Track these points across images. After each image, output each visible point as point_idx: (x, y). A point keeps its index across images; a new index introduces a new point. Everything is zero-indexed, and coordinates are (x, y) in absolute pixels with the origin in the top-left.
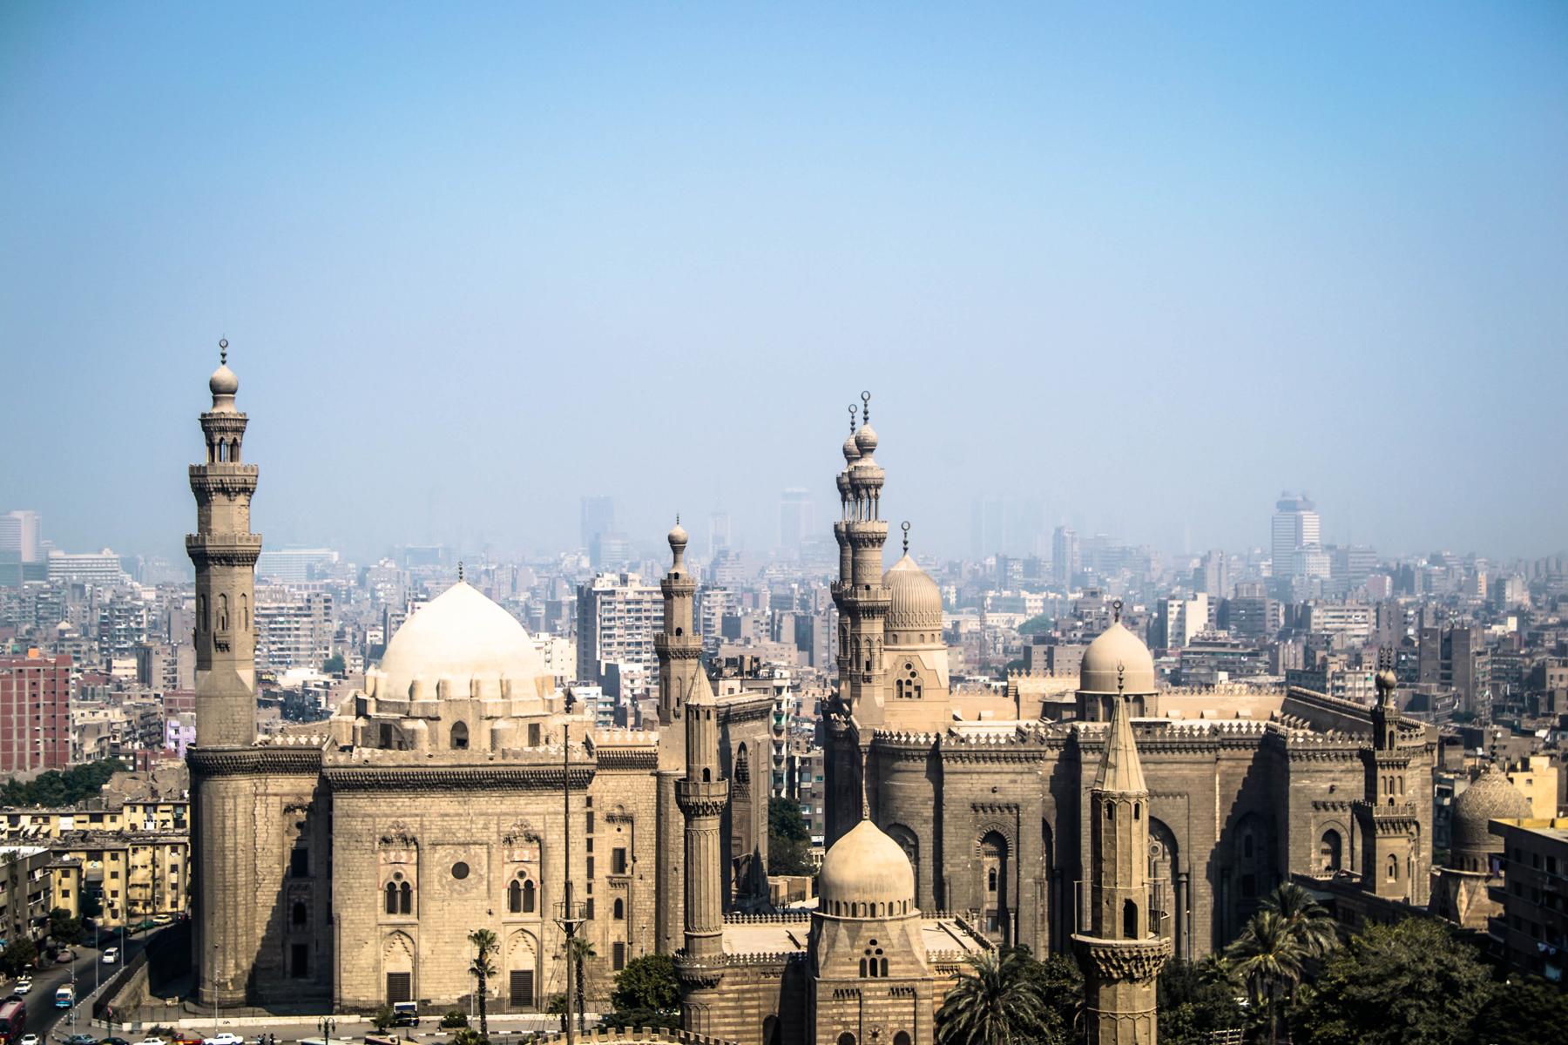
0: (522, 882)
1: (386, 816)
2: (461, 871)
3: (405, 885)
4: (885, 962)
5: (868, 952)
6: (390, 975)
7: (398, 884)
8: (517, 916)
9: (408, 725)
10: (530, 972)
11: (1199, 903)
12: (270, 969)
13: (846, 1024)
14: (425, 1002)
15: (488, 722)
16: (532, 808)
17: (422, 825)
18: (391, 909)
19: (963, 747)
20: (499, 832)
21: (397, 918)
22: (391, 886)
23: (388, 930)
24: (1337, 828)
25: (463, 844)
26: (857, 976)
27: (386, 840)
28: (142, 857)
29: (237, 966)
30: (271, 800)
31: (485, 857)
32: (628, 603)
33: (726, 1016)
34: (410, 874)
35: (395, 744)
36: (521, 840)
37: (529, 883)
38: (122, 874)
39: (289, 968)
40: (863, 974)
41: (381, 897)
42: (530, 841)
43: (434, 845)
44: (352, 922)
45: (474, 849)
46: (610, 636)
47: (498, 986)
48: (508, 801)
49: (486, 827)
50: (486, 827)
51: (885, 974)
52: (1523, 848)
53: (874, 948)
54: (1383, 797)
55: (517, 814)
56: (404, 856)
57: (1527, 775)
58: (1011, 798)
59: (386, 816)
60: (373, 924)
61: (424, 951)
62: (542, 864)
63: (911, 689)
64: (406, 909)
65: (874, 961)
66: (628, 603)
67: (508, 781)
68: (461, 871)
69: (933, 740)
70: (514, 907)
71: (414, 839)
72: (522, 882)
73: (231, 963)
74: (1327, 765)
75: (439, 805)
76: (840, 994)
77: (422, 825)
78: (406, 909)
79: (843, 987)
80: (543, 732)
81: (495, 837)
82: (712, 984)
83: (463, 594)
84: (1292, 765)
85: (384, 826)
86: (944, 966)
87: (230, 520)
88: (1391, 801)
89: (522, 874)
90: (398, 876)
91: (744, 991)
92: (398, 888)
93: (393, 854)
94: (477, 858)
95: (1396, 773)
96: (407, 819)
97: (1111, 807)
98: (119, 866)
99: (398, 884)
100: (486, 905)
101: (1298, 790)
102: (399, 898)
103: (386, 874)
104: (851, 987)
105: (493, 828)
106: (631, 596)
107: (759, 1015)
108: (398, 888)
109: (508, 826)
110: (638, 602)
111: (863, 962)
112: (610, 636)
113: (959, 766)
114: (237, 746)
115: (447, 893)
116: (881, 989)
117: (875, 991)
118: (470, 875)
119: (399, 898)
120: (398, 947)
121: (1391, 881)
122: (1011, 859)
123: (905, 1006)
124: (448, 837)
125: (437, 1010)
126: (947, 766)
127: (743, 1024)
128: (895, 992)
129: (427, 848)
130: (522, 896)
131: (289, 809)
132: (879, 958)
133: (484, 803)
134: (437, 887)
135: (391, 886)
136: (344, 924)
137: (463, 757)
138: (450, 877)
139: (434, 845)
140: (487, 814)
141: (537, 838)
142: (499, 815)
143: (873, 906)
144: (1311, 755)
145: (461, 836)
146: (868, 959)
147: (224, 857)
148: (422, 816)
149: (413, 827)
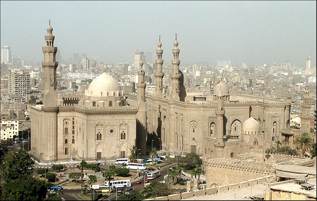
0: (123, 133)
1: (97, 120)
2: (112, 131)
3: (100, 134)
4: (258, 142)
5: (255, 140)
6: (97, 153)
9: (100, 102)
10: (124, 152)
12: (60, 153)
15: (116, 101)
16: (125, 119)
17: (104, 122)
18: (98, 140)
20: (119, 124)
23: (97, 143)
25: (112, 126)
26: (253, 145)
29: (55, 152)
30: (61, 118)
31: (116, 128)
33: (225, 153)
35: (96, 106)
39: (64, 153)
40: (254, 144)
43: (106, 126)
44: (90, 142)
46: (17, 84)
48: (121, 117)
49: (117, 122)
50: (117, 122)
53: (256, 140)
55: (123, 120)
59: (97, 120)
60: (95, 142)
61: (105, 148)
62: (128, 130)
65: (256, 142)
66: (21, 75)
67: (121, 113)
68: (112, 131)
70: (122, 139)
72: (123, 133)
73: (54, 152)
75: (108, 117)
77: (104, 122)
79: (251, 147)
81: (118, 124)
85: (97, 122)
87: (49, 59)
89: (123, 132)
90: (99, 132)
91: (227, 148)
92: (99, 135)
93: (98, 128)
96: (101, 121)
102: (99, 137)
103: (97, 133)
104: (252, 147)
105: (118, 122)
106: (22, 74)
107: (230, 153)
108: (99, 135)
109: (121, 122)
112: (17, 84)
115: (109, 136)
116: (257, 147)
118: (114, 132)
119: (99, 137)
124: (109, 124)
127: (228, 154)
129: (105, 127)
130: (123, 136)
132: (257, 141)
133: (117, 117)
137: (109, 109)
138: (110, 132)
139: (106, 126)
142: (119, 120)
146: (255, 142)
148: (104, 120)
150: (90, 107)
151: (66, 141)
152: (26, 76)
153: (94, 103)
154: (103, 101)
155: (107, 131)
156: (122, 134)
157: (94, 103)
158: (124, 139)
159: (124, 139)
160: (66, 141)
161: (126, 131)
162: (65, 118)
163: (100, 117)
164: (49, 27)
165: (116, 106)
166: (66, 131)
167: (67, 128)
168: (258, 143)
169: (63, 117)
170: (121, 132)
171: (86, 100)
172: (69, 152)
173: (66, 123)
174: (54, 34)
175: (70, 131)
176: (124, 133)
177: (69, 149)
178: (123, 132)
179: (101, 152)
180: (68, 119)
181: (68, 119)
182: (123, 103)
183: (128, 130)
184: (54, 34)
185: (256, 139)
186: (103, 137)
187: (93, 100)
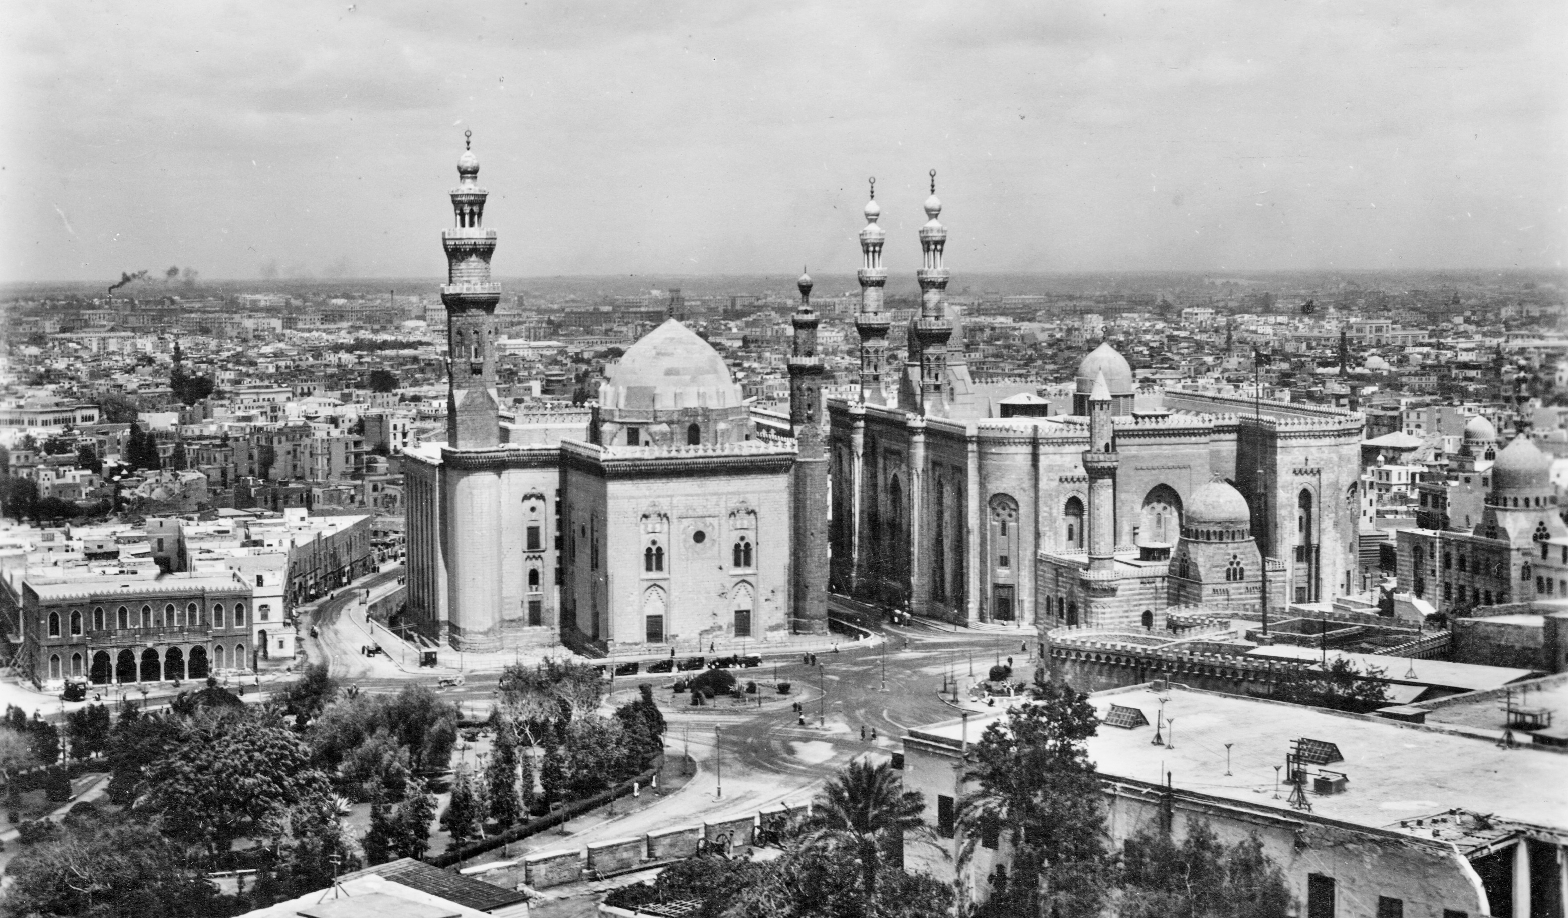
2: (699, 537)
3: (659, 549)
4: (1242, 570)
8: (740, 571)
16: (749, 489)
18: (649, 568)
21: (654, 575)
27: (645, 516)
36: (743, 512)
39: (527, 617)
40: (1228, 577)
42: (749, 513)
43: (680, 518)
45: (708, 520)
55: (739, 493)
64: (659, 568)
68: (699, 537)
70: (737, 564)
71: (665, 515)
78: (659, 568)
81: (723, 511)
82: (1112, 591)
89: (742, 538)
90: (654, 542)
99: (654, 548)
100: (718, 564)
102: (654, 558)
105: (722, 504)
109: (733, 504)
113: (1050, 449)
120: (654, 596)
122: (1085, 517)
124: (691, 513)
126: (1042, 449)
130: (743, 554)
131: (526, 497)
136: (616, 580)
139: (680, 518)
141: (753, 512)
144: (1289, 436)
148: (671, 496)
159: (747, 563)
160: (534, 578)
161: (751, 537)
167: (537, 528)
168: (1246, 573)
171: (604, 421)
180: (541, 497)
181: (541, 497)
185: (1235, 557)
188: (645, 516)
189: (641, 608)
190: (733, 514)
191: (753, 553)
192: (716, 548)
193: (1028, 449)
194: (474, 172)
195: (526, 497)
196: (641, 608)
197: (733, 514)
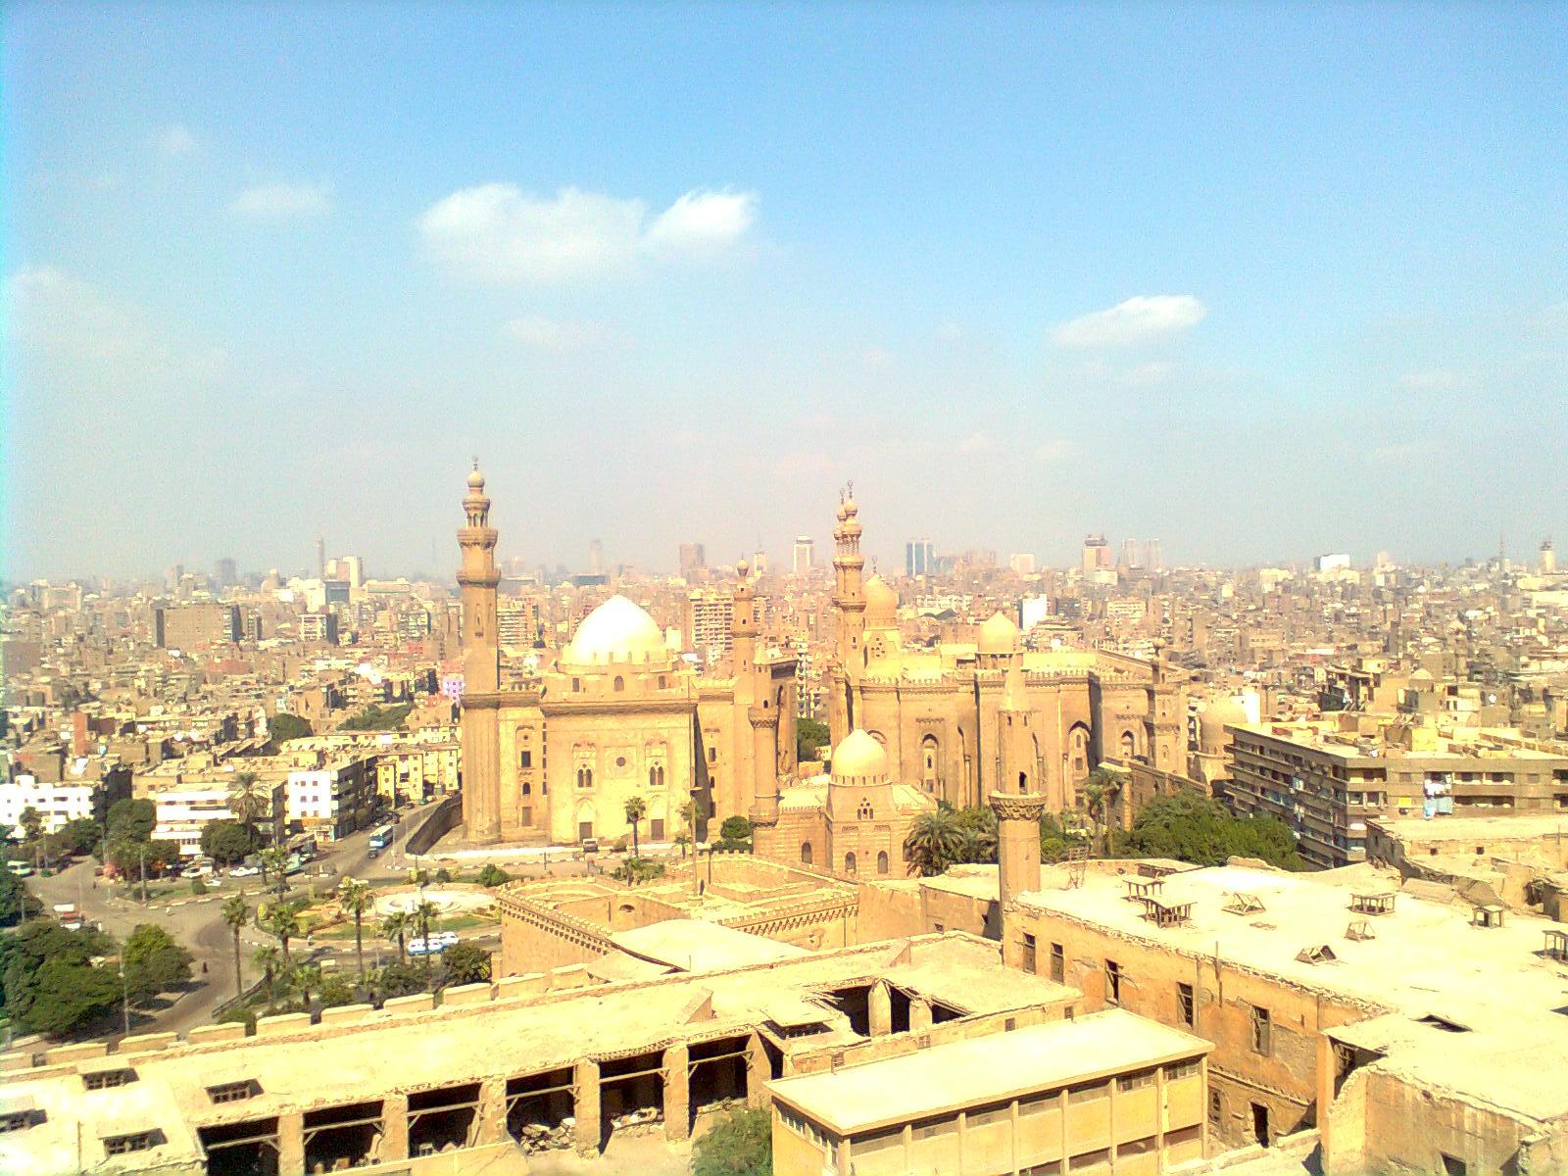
2: (621, 762)
3: (589, 771)
4: (871, 811)
7: (585, 770)
8: (654, 788)
11: (1050, 774)
13: (850, 846)
14: (601, 839)
16: (661, 725)
19: (911, 686)
22: (581, 772)
23: (579, 797)
24: (1132, 731)
27: (576, 745)
28: (432, 757)
32: (710, 605)
34: (592, 765)
35: (581, 689)
37: (661, 769)
38: (420, 768)
39: (520, 821)
41: (576, 778)
47: (644, 827)
49: (636, 735)
50: (636, 735)
51: (872, 817)
52: (1242, 741)
53: (865, 803)
54: (1158, 711)
56: (588, 754)
57: (1240, 698)
58: (940, 716)
63: (879, 652)
66: (710, 605)
68: (621, 762)
69: (894, 682)
70: (652, 782)
72: (657, 768)
74: (1125, 693)
75: (610, 723)
76: (845, 829)
78: (589, 784)
80: (667, 681)
81: (640, 742)
83: (618, 601)
84: (1103, 693)
85: (576, 737)
86: (905, 812)
88: (1164, 714)
89: (656, 763)
90: (585, 766)
94: (631, 754)
95: (1167, 697)
96: (590, 733)
97: (1010, 718)
98: (418, 764)
99: (585, 770)
100: (636, 782)
101: (1107, 709)
102: (585, 778)
105: (640, 737)
106: (712, 602)
109: (648, 736)
110: (716, 605)
111: (859, 811)
114: (488, 692)
117: (866, 825)
119: (585, 778)
121: (1165, 760)
123: (884, 835)
125: (609, 843)
128: (879, 828)
130: (657, 776)
131: (519, 728)
132: (868, 808)
134: (608, 771)
135: (581, 772)
138: (616, 765)
140: (633, 729)
143: (864, 779)
144: (1114, 687)
145: (621, 741)
146: (862, 809)
147: (482, 758)
149: (592, 737)
150: (16, 716)
151: (527, 789)
152: (723, 607)
153: (576, 684)
154: (596, 678)
155: (607, 762)
156: (652, 769)
157: (576, 681)
158: (661, 782)
159: (661, 782)
160: (527, 789)
162: (521, 724)
163: (586, 722)
164: (474, 476)
165: (632, 693)
166: (526, 758)
169: (515, 720)
170: (650, 763)
172: (535, 817)
173: (526, 738)
174: (487, 494)
175: (535, 761)
176: (661, 769)
177: (534, 811)
178: (656, 763)
179: (590, 824)
180: (531, 728)
181: (531, 728)
182: (662, 682)
183: (670, 756)
184: (487, 494)
185: (865, 799)
186: (595, 777)
187: (576, 672)
188: (576, 745)
189: (575, 816)
190: (648, 744)
191: (666, 774)
192: (635, 771)
193: (895, 694)
194: (481, 486)
195: (519, 728)
196: (575, 816)
197: (648, 744)
